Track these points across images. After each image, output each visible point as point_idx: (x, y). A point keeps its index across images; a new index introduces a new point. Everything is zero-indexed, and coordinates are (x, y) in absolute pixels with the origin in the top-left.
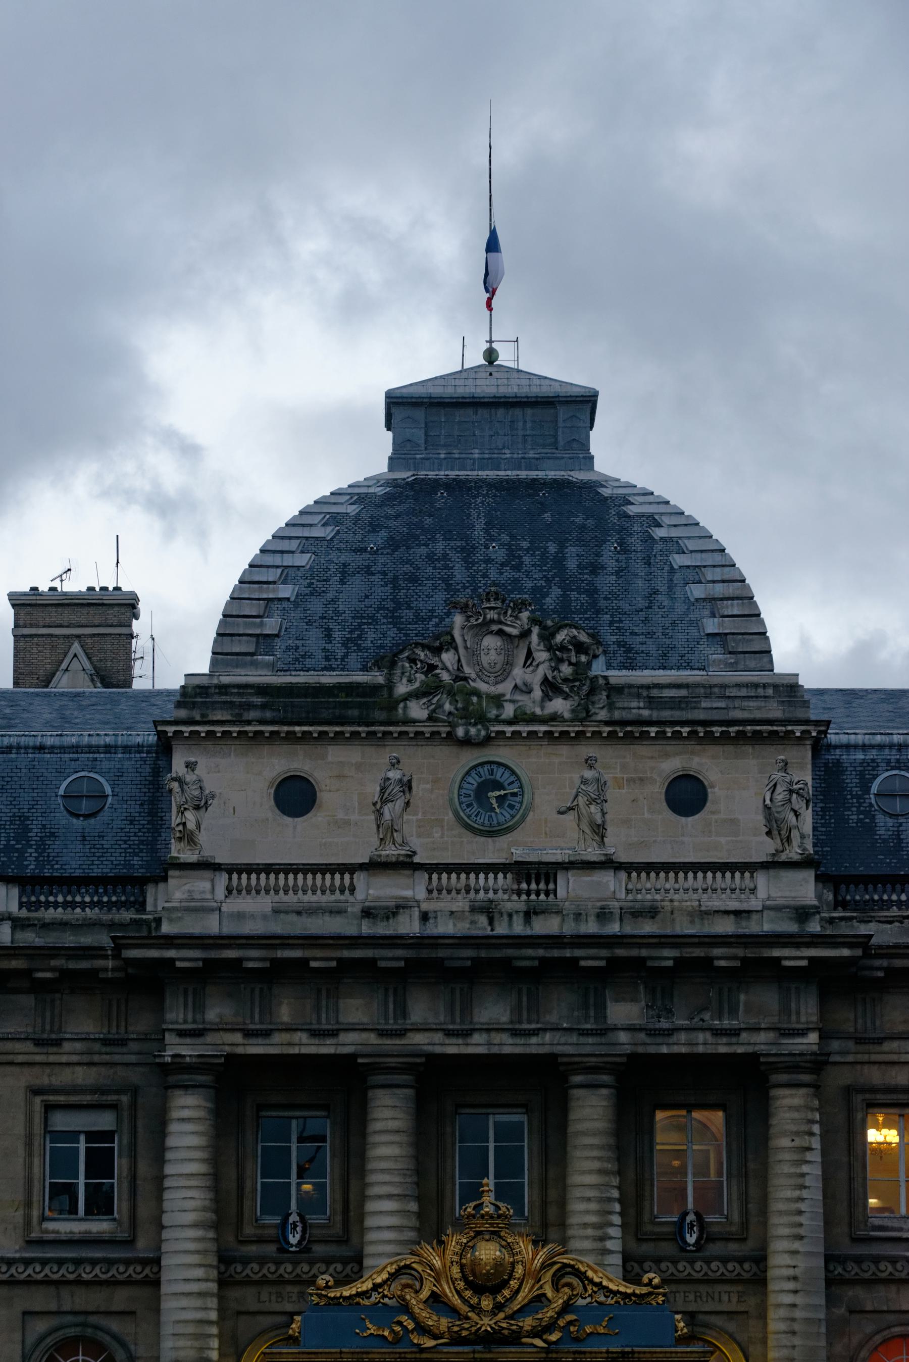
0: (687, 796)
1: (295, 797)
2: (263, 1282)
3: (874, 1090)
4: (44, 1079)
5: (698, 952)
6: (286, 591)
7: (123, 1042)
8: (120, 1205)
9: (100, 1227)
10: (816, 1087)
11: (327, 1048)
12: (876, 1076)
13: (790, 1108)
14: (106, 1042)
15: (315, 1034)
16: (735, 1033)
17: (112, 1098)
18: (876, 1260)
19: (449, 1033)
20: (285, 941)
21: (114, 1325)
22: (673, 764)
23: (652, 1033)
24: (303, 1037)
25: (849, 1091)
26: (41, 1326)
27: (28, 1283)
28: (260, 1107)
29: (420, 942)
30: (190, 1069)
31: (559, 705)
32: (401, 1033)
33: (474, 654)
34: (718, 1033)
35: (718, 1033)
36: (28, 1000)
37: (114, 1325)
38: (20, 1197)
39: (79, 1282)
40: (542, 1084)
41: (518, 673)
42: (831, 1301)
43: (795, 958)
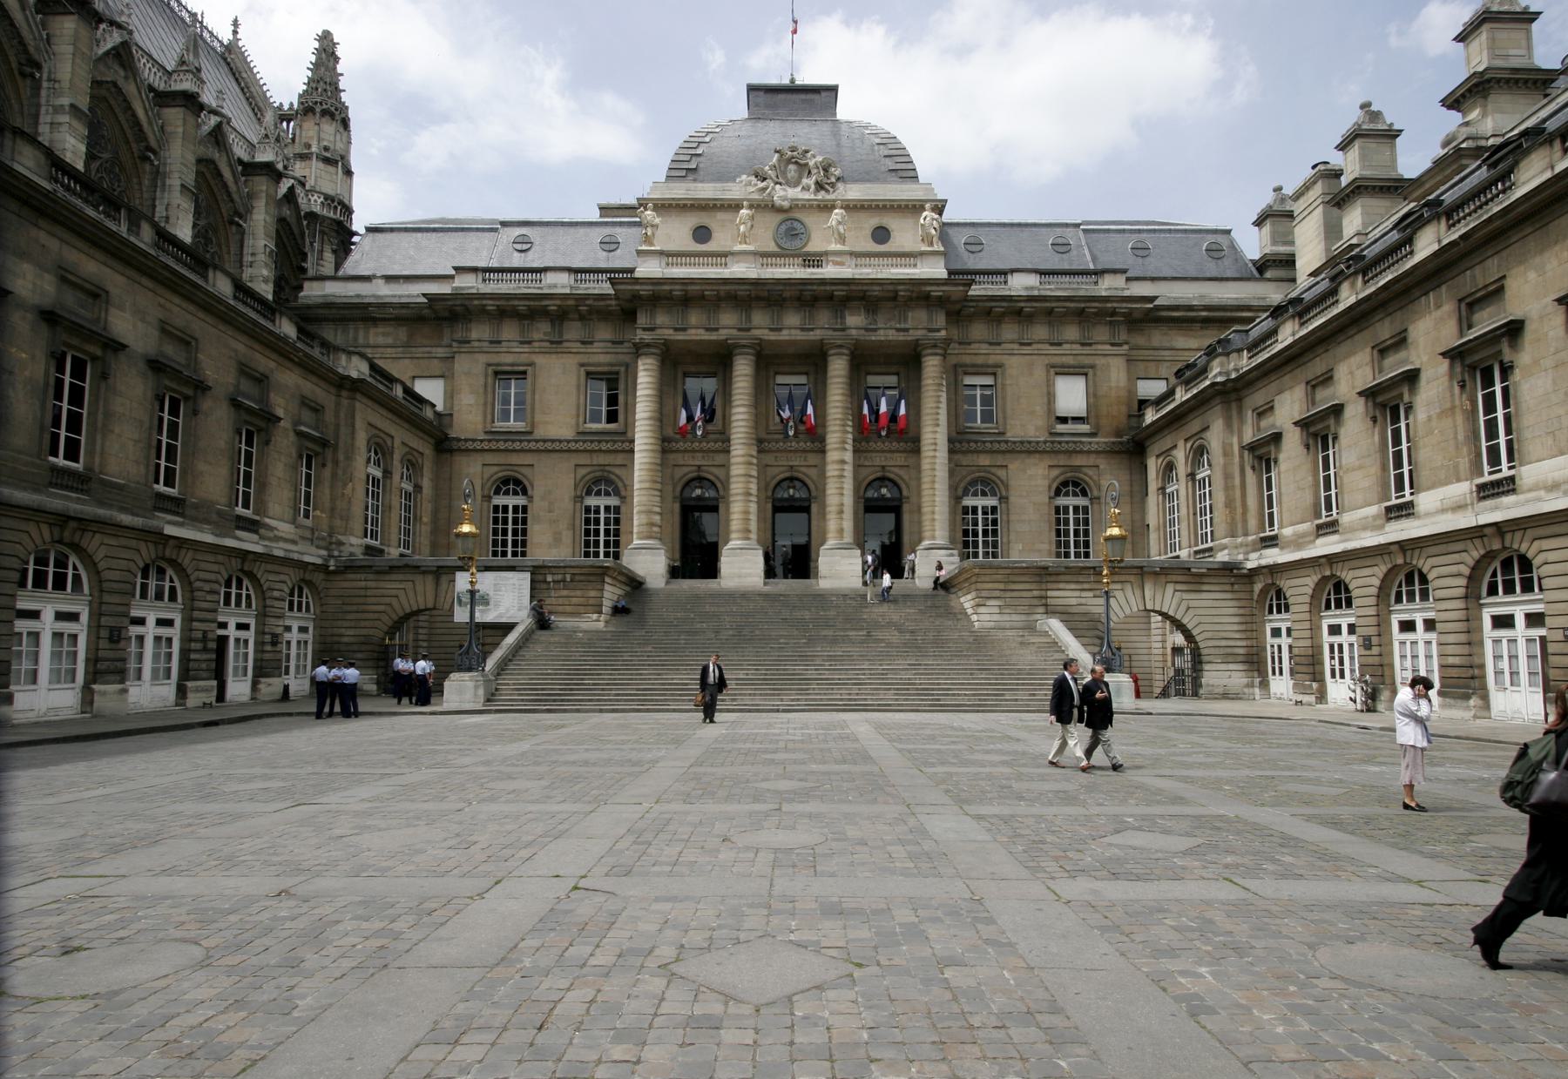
0: (881, 234)
1: (702, 234)
2: (686, 451)
3: (966, 366)
4: (584, 359)
5: (891, 288)
6: (699, 151)
7: (621, 343)
8: (621, 417)
9: (612, 426)
10: (944, 356)
11: (713, 337)
12: (967, 360)
13: (932, 366)
14: (614, 342)
15: (707, 329)
16: (906, 330)
17: (616, 369)
18: (969, 442)
19: (771, 330)
20: (692, 281)
21: (617, 471)
22: (875, 221)
23: (867, 330)
24: (702, 331)
25: (955, 366)
26: (582, 471)
27: (577, 451)
28: (686, 375)
29: (757, 283)
30: (648, 345)
31: (821, 195)
32: (748, 330)
33: (784, 173)
34: (898, 330)
35: (898, 330)
36: (579, 324)
37: (617, 471)
38: (574, 412)
39: (600, 451)
40: (813, 360)
41: (805, 181)
42: (950, 460)
43: (936, 292)
